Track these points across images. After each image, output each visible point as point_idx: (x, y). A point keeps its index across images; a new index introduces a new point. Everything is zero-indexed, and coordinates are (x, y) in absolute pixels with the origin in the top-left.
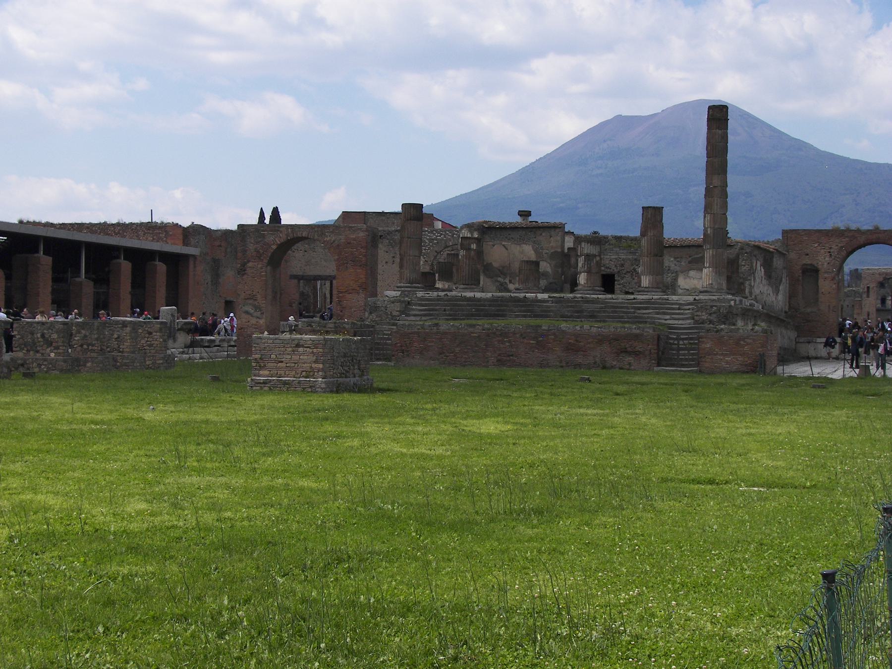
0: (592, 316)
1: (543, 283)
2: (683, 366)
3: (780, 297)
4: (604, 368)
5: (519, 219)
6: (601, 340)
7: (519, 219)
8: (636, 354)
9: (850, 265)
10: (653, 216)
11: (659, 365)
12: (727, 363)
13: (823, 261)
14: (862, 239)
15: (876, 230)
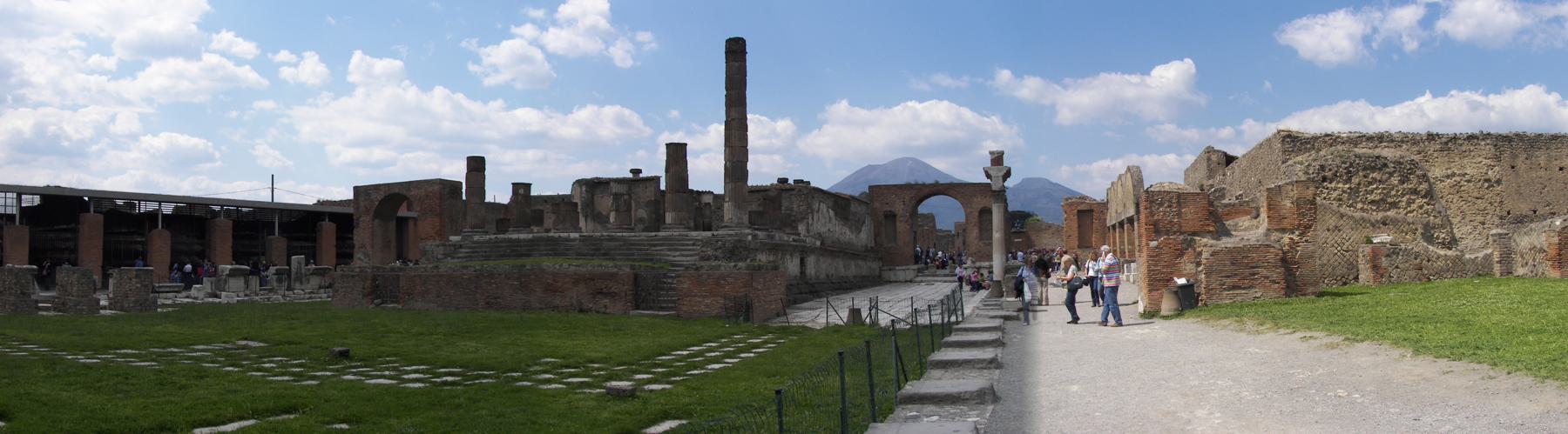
0: (606, 255)
1: (641, 226)
2: (662, 309)
3: (863, 235)
4: (581, 311)
5: (631, 176)
6: (578, 279)
7: (631, 176)
8: (613, 295)
9: (922, 209)
10: (677, 154)
11: (637, 307)
12: (707, 306)
13: (899, 208)
14: (926, 191)
15: (937, 184)
